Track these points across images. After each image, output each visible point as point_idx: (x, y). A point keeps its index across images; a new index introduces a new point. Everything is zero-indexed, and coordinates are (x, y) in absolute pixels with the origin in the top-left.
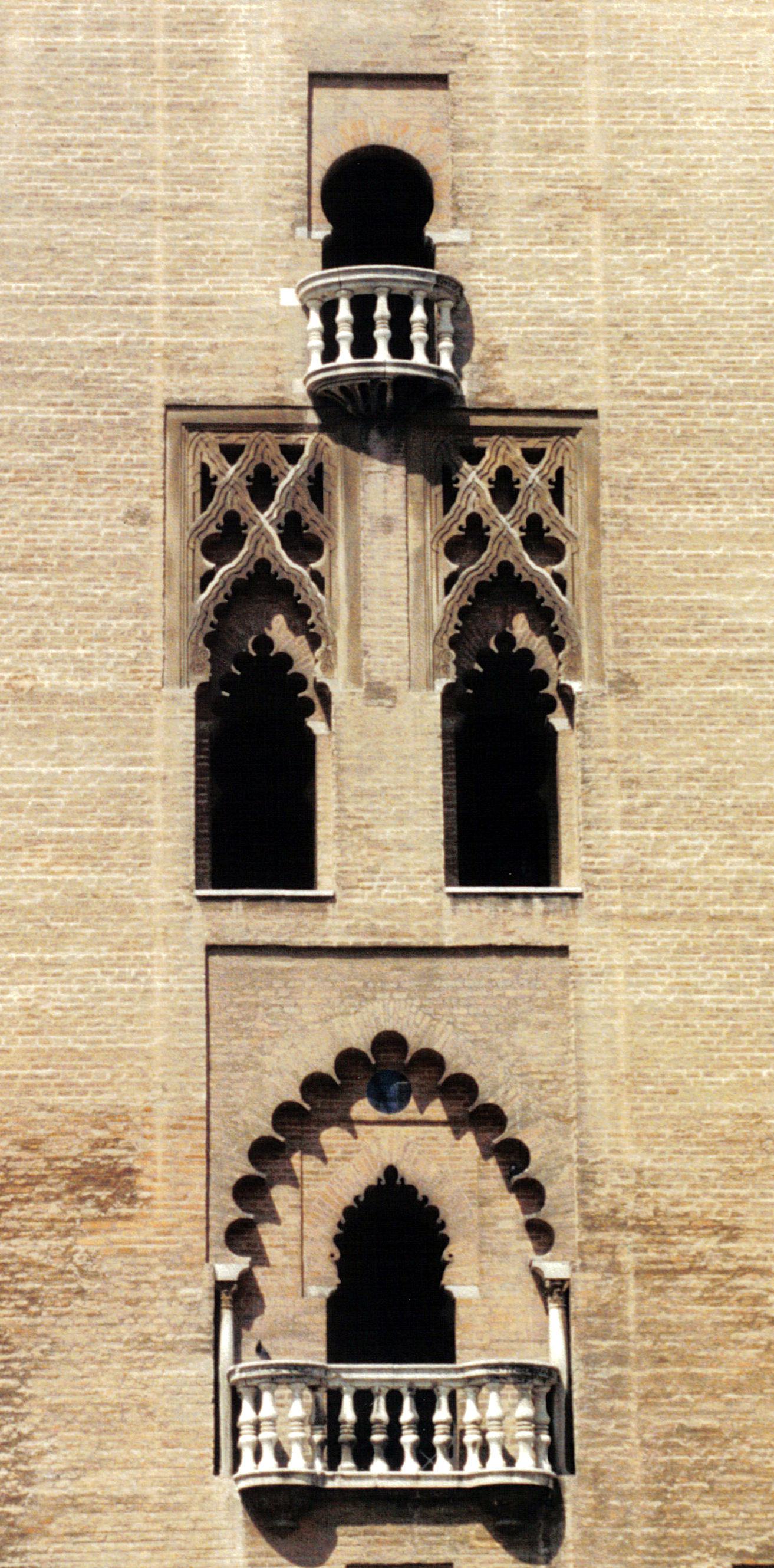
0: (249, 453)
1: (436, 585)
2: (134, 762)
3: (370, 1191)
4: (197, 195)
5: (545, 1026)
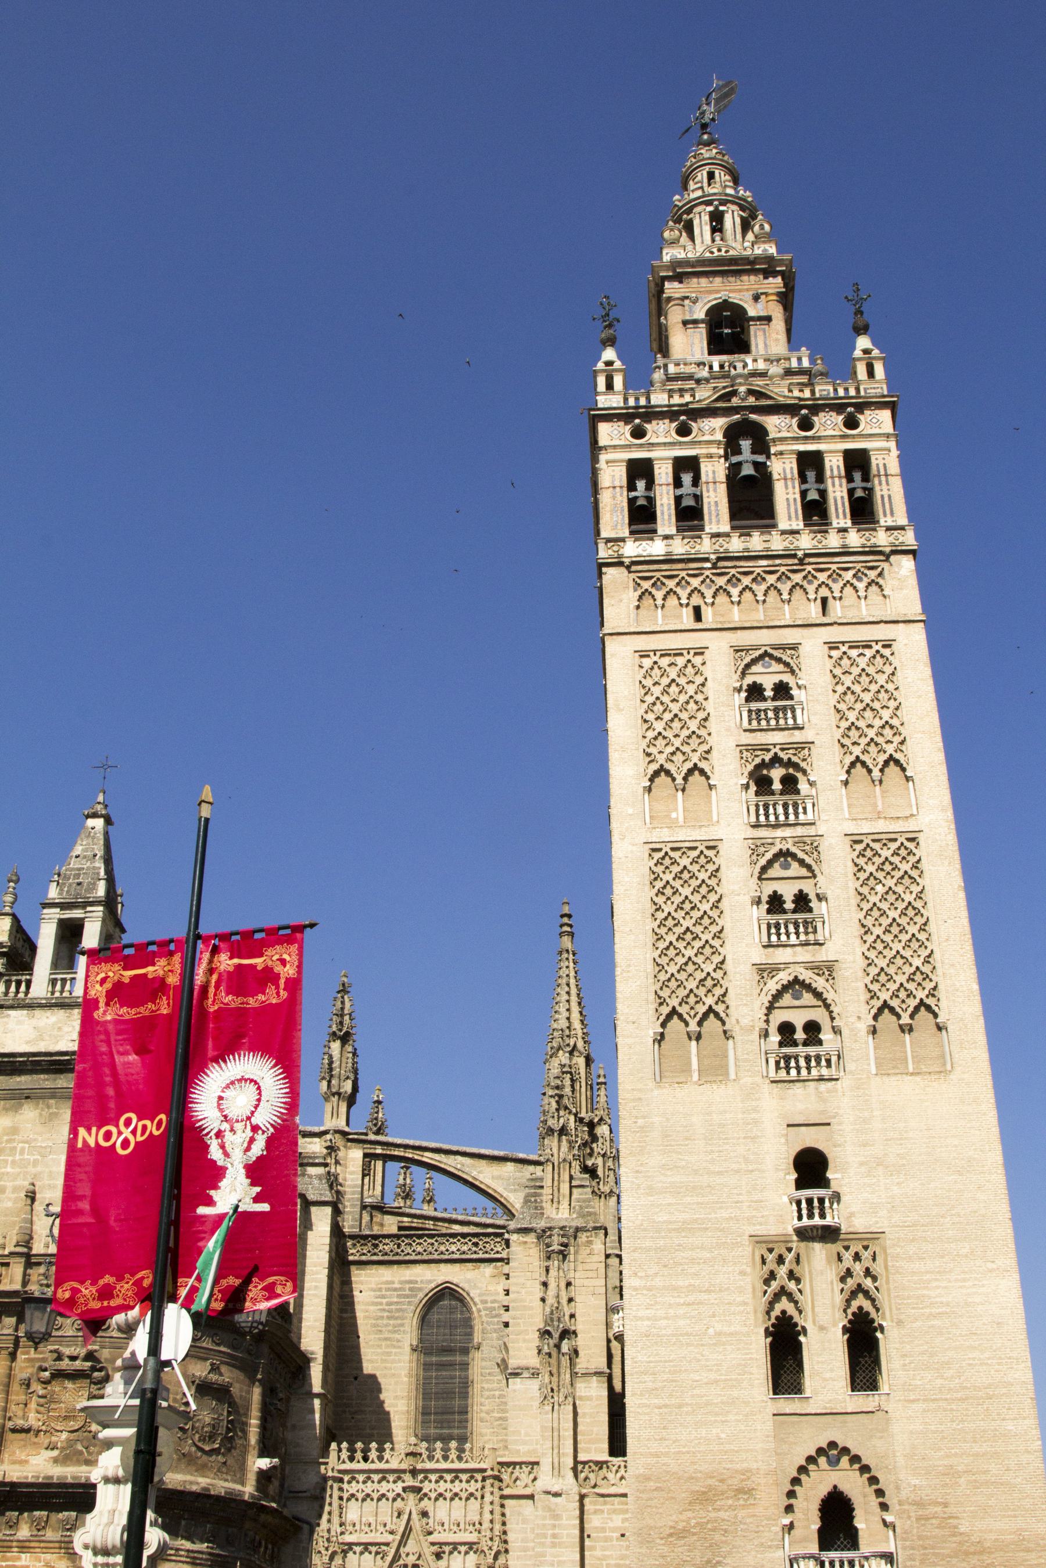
0: (776, 1251)
1: (837, 1291)
2: (747, 1354)
3: (829, 1493)
4: (755, 1166)
5: (882, 1437)
